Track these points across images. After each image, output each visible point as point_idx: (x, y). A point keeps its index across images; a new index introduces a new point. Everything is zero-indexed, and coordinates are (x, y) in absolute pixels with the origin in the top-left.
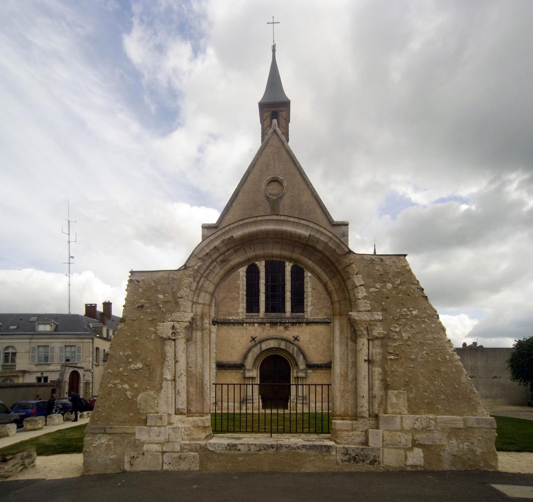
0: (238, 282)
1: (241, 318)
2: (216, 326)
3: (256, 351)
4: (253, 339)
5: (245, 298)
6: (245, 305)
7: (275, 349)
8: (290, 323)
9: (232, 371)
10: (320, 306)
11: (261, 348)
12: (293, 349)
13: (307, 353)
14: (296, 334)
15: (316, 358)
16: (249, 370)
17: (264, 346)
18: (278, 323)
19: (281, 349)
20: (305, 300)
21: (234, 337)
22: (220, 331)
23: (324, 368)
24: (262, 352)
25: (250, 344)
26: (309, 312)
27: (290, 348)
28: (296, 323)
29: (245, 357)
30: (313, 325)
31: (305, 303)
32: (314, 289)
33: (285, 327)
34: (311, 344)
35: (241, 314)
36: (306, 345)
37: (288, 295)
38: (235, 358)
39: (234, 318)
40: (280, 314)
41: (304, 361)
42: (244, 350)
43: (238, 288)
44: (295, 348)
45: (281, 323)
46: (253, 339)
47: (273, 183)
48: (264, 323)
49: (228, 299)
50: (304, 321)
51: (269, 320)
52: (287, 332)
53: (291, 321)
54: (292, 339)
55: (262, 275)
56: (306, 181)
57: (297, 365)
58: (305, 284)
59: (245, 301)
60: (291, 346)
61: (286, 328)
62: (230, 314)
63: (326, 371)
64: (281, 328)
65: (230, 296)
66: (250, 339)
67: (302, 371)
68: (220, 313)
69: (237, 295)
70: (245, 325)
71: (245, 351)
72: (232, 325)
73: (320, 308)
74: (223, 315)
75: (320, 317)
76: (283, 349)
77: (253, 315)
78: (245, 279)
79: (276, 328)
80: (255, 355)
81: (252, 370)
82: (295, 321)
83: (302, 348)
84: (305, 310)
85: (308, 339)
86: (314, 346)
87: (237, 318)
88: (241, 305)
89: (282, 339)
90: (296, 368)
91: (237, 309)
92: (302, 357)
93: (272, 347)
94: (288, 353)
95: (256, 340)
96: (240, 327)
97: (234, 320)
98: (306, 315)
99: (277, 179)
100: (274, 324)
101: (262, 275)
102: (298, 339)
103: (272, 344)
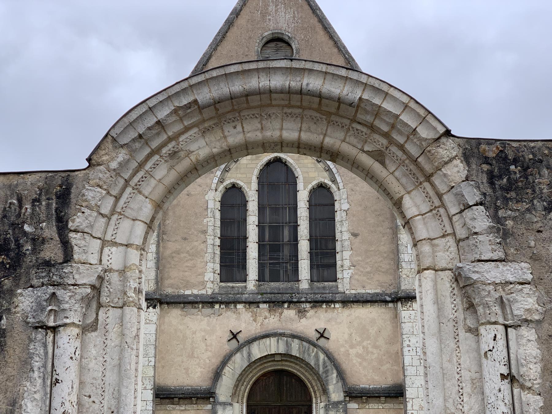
0: (205, 221)
1: (210, 292)
2: (158, 309)
3: (239, 362)
4: (234, 336)
5: (218, 251)
6: (218, 267)
7: (278, 358)
8: (310, 302)
9: (188, 407)
10: (369, 269)
11: (249, 354)
12: (317, 357)
13: (345, 366)
14: (321, 326)
15: (366, 377)
16: (224, 404)
17: (258, 351)
18: (284, 302)
19: (291, 356)
20: (338, 256)
21: (194, 333)
22: (167, 320)
23: (383, 399)
24: (252, 364)
25: (227, 348)
26: (346, 281)
27: (309, 355)
28: (323, 302)
29: (217, 375)
30: (355, 306)
31: (339, 263)
32: (355, 235)
33: (299, 312)
34: (352, 346)
35: (209, 285)
36: (342, 350)
37: (304, 246)
38: (195, 376)
39: (195, 292)
40: (289, 285)
41: (340, 384)
42: (214, 360)
43: (205, 232)
44: (322, 356)
45: (290, 302)
46: (234, 336)
47: (272, 45)
48: (256, 303)
49: (182, 255)
50: (338, 297)
51: (267, 297)
52: (303, 320)
53: (311, 297)
54: (314, 336)
55: (253, 206)
56: (334, 40)
57: (325, 391)
58: (338, 225)
59: (218, 259)
60: (313, 351)
61: (302, 313)
62: (187, 287)
63: (387, 406)
64: (290, 313)
65: (188, 248)
66: (228, 336)
67: (336, 404)
68: (167, 282)
69: (202, 246)
70: (217, 306)
71: (216, 362)
72: (190, 306)
73: (368, 273)
74: (172, 286)
75: (371, 289)
76: (296, 358)
77: (233, 287)
78: (218, 215)
79: (281, 314)
80: (239, 372)
81: (231, 404)
82: (318, 297)
83: (336, 356)
84: (339, 275)
85: (346, 336)
86: (360, 350)
87: (201, 292)
88: (210, 265)
89: (294, 336)
90: (323, 398)
91: (203, 274)
92: (335, 375)
93: (273, 352)
94: (307, 364)
95: (241, 337)
96: (207, 311)
97: (196, 296)
98: (340, 286)
99: (280, 36)
100: (275, 304)
101: (253, 206)
102: (325, 335)
103: (272, 346)
